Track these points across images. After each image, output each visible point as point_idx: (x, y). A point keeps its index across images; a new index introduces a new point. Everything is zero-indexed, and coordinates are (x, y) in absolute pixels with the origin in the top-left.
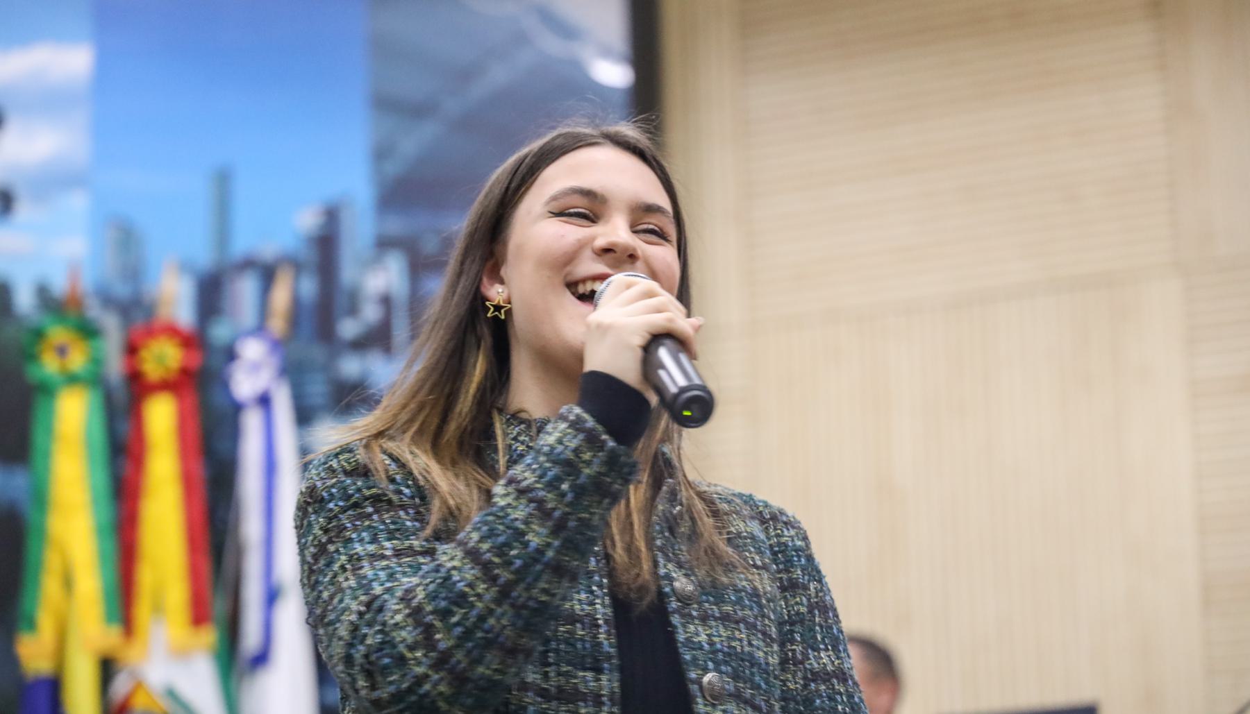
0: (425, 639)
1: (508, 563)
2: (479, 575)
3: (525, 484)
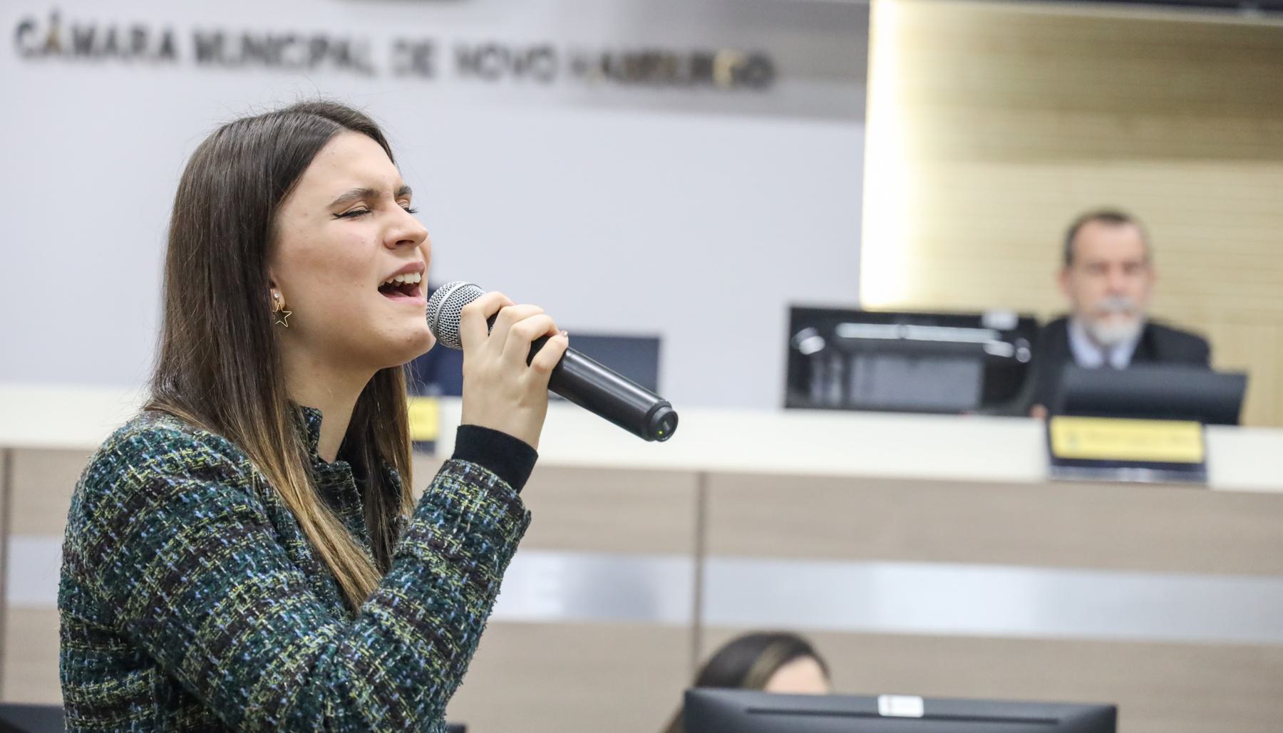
2: (435, 651)
3: (453, 551)
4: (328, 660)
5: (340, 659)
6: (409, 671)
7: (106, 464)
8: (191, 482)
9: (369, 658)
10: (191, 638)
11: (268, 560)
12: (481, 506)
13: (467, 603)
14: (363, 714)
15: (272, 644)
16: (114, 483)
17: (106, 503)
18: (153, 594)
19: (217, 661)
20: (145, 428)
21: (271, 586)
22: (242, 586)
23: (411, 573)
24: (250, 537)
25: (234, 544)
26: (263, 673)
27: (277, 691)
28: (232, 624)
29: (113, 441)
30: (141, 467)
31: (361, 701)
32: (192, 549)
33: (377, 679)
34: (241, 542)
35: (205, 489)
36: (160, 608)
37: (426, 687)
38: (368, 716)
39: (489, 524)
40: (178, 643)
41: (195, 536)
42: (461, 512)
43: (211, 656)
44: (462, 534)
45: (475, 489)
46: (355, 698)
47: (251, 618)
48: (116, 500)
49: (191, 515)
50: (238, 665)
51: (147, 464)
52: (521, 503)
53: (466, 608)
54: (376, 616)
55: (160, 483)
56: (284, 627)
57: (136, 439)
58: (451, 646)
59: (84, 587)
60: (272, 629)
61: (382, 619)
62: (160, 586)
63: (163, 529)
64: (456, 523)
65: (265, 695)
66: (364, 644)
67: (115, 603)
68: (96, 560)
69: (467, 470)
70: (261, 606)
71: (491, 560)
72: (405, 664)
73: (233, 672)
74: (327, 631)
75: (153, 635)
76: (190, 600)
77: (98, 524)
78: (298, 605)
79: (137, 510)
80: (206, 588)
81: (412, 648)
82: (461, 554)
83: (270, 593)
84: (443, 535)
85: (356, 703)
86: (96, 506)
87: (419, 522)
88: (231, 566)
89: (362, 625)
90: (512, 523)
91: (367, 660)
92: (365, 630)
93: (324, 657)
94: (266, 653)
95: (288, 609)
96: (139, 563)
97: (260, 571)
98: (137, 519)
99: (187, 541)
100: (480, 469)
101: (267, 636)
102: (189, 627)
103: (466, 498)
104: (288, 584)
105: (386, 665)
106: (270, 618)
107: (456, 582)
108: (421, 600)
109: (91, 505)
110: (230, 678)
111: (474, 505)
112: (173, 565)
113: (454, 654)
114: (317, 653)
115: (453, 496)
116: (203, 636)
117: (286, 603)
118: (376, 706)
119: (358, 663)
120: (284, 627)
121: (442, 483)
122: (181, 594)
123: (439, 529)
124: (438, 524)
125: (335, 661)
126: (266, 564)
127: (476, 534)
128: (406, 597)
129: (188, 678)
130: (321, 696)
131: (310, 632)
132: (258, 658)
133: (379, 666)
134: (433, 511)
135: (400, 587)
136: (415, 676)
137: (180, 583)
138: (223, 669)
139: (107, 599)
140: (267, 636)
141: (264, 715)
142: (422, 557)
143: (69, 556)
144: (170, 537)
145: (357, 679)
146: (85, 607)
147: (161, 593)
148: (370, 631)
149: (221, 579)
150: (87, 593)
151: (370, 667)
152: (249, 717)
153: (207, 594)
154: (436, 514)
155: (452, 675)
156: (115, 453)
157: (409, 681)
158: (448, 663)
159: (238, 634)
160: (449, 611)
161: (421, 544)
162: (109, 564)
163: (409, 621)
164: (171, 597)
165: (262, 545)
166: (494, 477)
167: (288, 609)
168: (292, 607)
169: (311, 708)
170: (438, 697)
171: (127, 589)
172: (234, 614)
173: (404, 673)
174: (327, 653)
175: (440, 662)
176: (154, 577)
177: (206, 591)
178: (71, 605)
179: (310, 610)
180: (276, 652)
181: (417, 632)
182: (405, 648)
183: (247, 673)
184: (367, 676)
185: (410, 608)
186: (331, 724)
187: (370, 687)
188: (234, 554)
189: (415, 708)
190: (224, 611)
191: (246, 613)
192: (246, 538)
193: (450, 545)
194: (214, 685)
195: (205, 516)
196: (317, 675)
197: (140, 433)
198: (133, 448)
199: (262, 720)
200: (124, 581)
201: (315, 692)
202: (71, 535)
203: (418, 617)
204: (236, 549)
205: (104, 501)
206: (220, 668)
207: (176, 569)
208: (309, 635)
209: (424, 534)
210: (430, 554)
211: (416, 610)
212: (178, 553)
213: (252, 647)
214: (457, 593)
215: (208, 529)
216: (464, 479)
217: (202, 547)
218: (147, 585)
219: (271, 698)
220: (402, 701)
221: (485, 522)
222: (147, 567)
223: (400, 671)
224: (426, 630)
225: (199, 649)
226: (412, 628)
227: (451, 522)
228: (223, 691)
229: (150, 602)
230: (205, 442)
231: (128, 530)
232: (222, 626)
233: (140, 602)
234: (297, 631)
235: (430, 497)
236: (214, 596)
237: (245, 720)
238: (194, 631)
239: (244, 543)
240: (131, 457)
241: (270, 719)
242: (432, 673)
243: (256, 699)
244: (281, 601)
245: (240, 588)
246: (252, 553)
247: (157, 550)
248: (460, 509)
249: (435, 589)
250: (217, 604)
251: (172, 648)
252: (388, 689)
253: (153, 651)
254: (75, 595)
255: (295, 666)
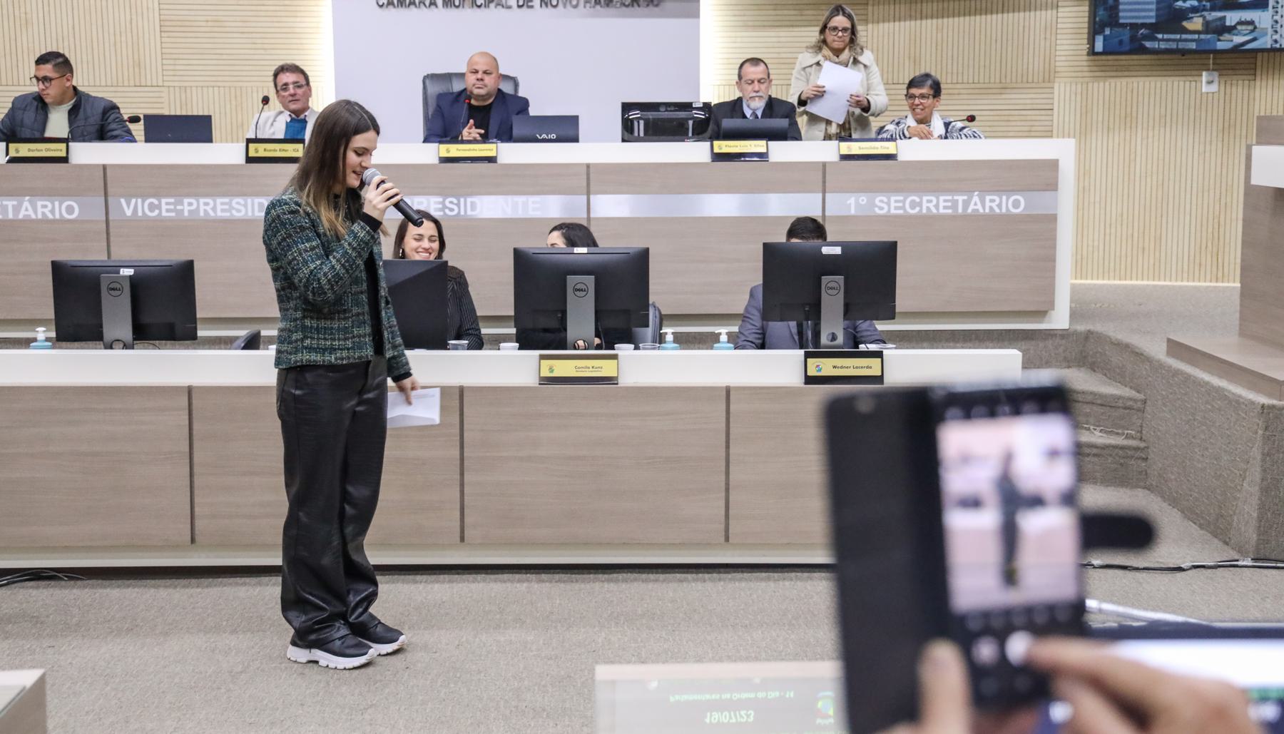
1: (352, 269)
70: (301, 254)
107: (354, 254)
166: (368, 228)
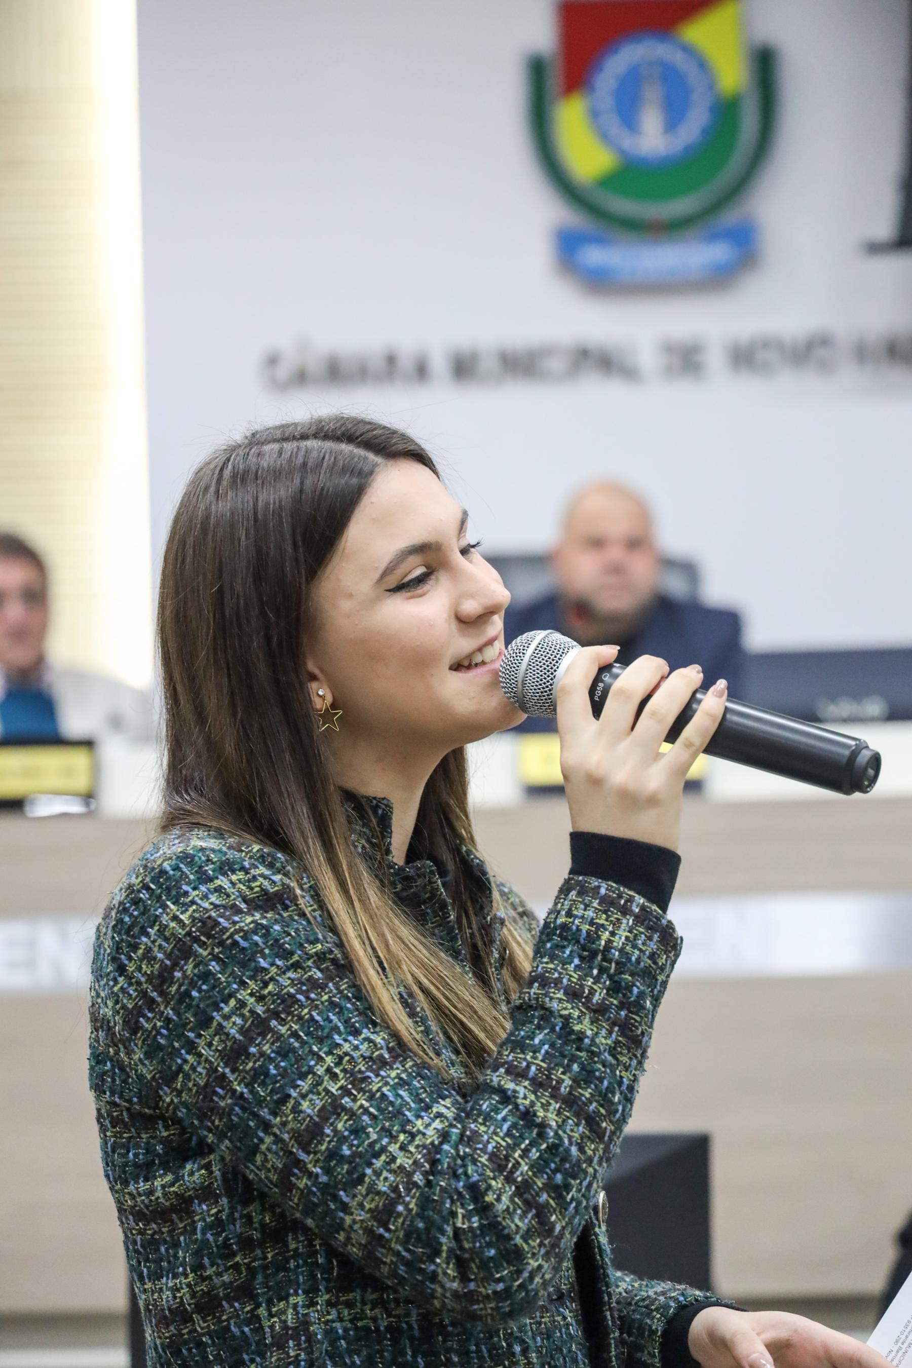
0: (539, 1223)
2: (587, 1132)
3: (596, 998)
4: (452, 1151)
5: (467, 1150)
6: (558, 1163)
7: (136, 902)
8: (249, 919)
9: (506, 1149)
10: (267, 1127)
11: (356, 1016)
12: (627, 938)
13: (618, 1065)
14: (504, 1223)
15: (377, 1133)
16: (152, 927)
17: (143, 954)
18: (212, 1070)
19: (306, 1156)
20: (180, 850)
21: (367, 1054)
22: (330, 1057)
23: (546, 1031)
24: (332, 988)
25: (313, 1000)
26: (369, 1171)
27: (388, 1195)
28: (323, 1108)
29: (142, 871)
30: (184, 904)
31: (501, 1207)
32: (260, 1009)
33: (518, 1176)
34: (322, 996)
35: (267, 928)
36: (223, 1088)
37: (578, 1181)
38: (510, 1227)
39: (638, 961)
40: (248, 1133)
41: (262, 992)
42: (601, 948)
43: (297, 1150)
44: (605, 976)
45: (616, 916)
46: (492, 1204)
47: (347, 1099)
48: (156, 949)
49: (253, 964)
50: (334, 1162)
51: (190, 898)
52: (674, 929)
53: (618, 1072)
54: (509, 1093)
55: (210, 923)
56: (390, 1109)
57: (171, 866)
58: (604, 1125)
59: (118, 1061)
60: (376, 1113)
61: (518, 1098)
62: (222, 1060)
63: (219, 985)
64: (596, 962)
65: (373, 1200)
66: (499, 1130)
67: (160, 1081)
68: (134, 1028)
69: (603, 891)
70: (358, 1081)
71: (643, 1007)
72: (552, 1154)
73: (328, 1171)
74: (443, 1110)
75: (213, 1123)
76: (262, 1077)
77: (134, 980)
78: (404, 1076)
79: (182, 962)
80: (283, 1061)
81: (560, 1132)
82: (607, 1002)
83: (367, 1063)
84: (580, 979)
85: (494, 1210)
86: (130, 959)
87: (547, 963)
88: (312, 1029)
89: (491, 1104)
90: (665, 957)
91: (504, 1152)
92: (497, 1111)
93: (446, 1147)
94: (372, 1145)
95: (392, 1083)
96: (191, 1030)
97: (350, 1033)
98: (184, 972)
99: (252, 1000)
100: (619, 890)
101: (369, 1122)
102: (265, 1113)
103: (606, 929)
104: (388, 1048)
105: (528, 1157)
106: (371, 1098)
108: (564, 1068)
109: (123, 957)
110: (324, 1179)
111: (617, 937)
112: (238, 1032)
113: (608, 1134)
114: (436, 1142)
115: (588, 927)
116: (284, 1124)
117: (389, 1076)
118: (519, 1212)
119: (493, 1157)
120: (390, 1109)
121: (570, 910)
122: (251, 1070)
123: (575, 971)
124: (573, 965)
125: (461, 1153)
126: (356, 1022)
127: (623, 976)
128: (544, 1065)
129: (263, 1177)
130: (448, 1201)
131: (423, 1114)
132: (361, 1152)
133: (520, 1160)
134: (564, 947)
135: (534, 1052)
136: (566, 1169)
137: (248, 1056)
138: (315, 1166)
139: (149, 1077)
140: (369, 1122)
141: (373, 1226)
142: (559, 1011)
143: (98, 1023)
144: (231, 996)
145: (494, 1178)
146: (122, 1087)
147: (222, 1068)
148: (504, 1113)
149: (301, 1047)
150: (122, 1069)
151: (508, 1161)
152: (351, 1227)
153: (285, 1069)
154: (568, 952)
155: (604, 1160)
156: (146, 887)
157: (559, 1177)
158: (602, 1146)
159: (331, 1121)
160: (601, 1080)
161: (554, 993)
162: (151, 1032)
163: (553, 1096)
164: (237, 1073)
165: (348, 997)
167: (392, 1083)
168: (396, 1080)
169: (436, 1216)
170: (589, 1191)
171: (177, 1063)
172: (323, 1094)
173: (553, 1166)
174: (449, 1142)
175: (593, 1146)
176: (213, 1048)
177: (282, 1064)
178: (103, 1085)
179: (419, 1082)
180: (384, 1143)
181: (564, 1110)
182: (552, 1134)
183: (347, 1172)
184: (505, 1174)
185: (552, 1079)
186: (463, 1237)
187: (510, 1188)
188: (314, 1013)
189: (566, 1209)
190: (310, 1091)
191: (340, 1092)
192: (327, 990)
193: (592, 992)
194: (302, 1186)
195: (272, 964)
196: (441, 1173)
197: (174, 857)
198: (169, 878)
199: (369, 1231)
200: (171, 1053)
201: (441, 1196)
202: (98, 995)
203: (562, 1089)
204: (316, 1007)
205: (141, 951)
206: (310, 1166)
207: (241, 1038)
208: (422, 1118)
209: (556, 979)
210: (569, 1006)
211: (560, 1082)
212: (242, 1016)
213: (352, 1137)
214: (606, 1054)
215: (278, 981)
216: (600, 904)
217: (272, 1007)
218: (203, 1059)
219: (381, 1204)
220: (552, 1202)
221: (633, 959)
222: (202, 1035)
223: (547, 1163)
224: (575, 1108)
225: (278, 1140)
226: (558, 1106)
227: (589, 961)
228: (314, 1194)
229: (208, 1080)
230: (257, 860)
231: (174, 989)
232: (309, 1111)
233: (195, 1080)
234: (407, 1113)
235: (555, 928)
236: (295, 1070)
237: (344, 1230)
238: (271, 1118)
239: (326, 997)
240: (169, 889)
241: (381, 1230)
242: (585, 1162)
243: (361, 1205)
244: (382, 1073)
245: (329, 1060)
246: (337, 1010)
247: (215, 1014)
248: (600, 945)
249: (581, 1052)
250: (299, 1082)
251: (240, 1140)
252: (534, 1189)
253: (212, 1142)
254: (108, 1071)
255: (410, 1162)
